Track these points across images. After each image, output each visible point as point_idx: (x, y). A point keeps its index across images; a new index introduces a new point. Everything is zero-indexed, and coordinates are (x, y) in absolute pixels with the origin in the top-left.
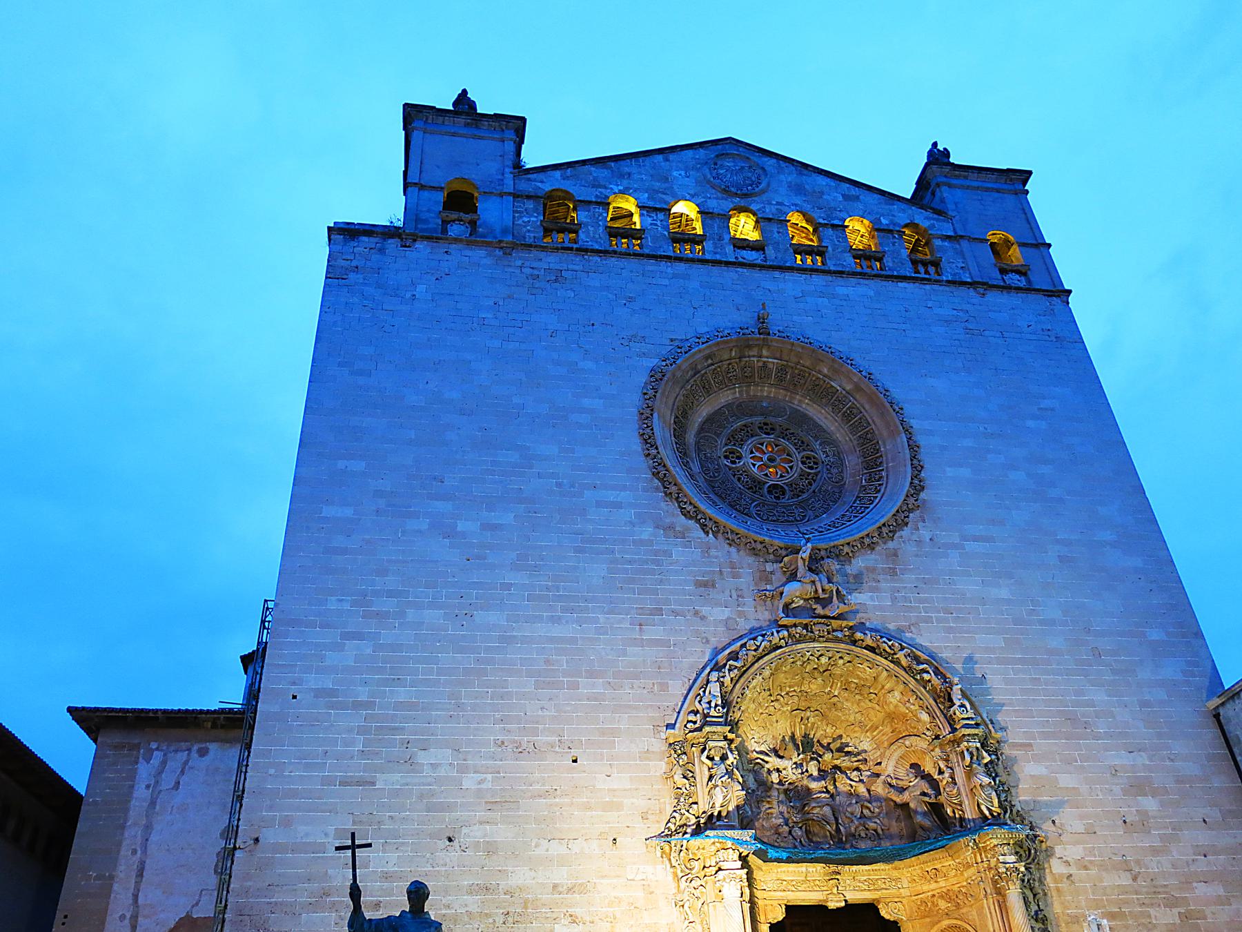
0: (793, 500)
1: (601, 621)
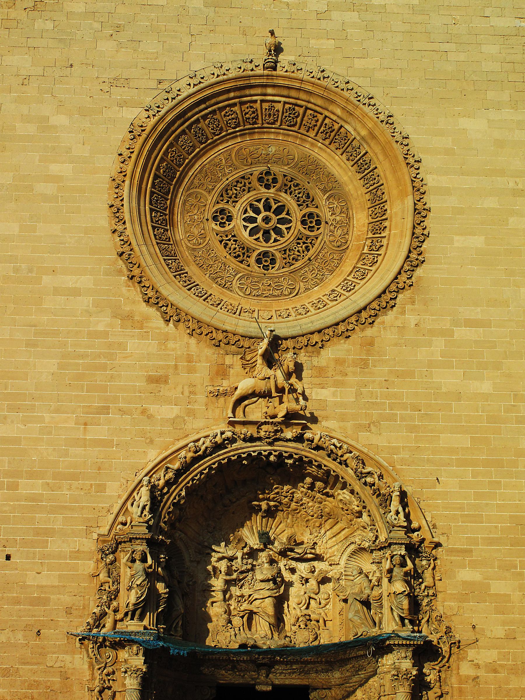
0: (284, 270)
1: (47, 420)
